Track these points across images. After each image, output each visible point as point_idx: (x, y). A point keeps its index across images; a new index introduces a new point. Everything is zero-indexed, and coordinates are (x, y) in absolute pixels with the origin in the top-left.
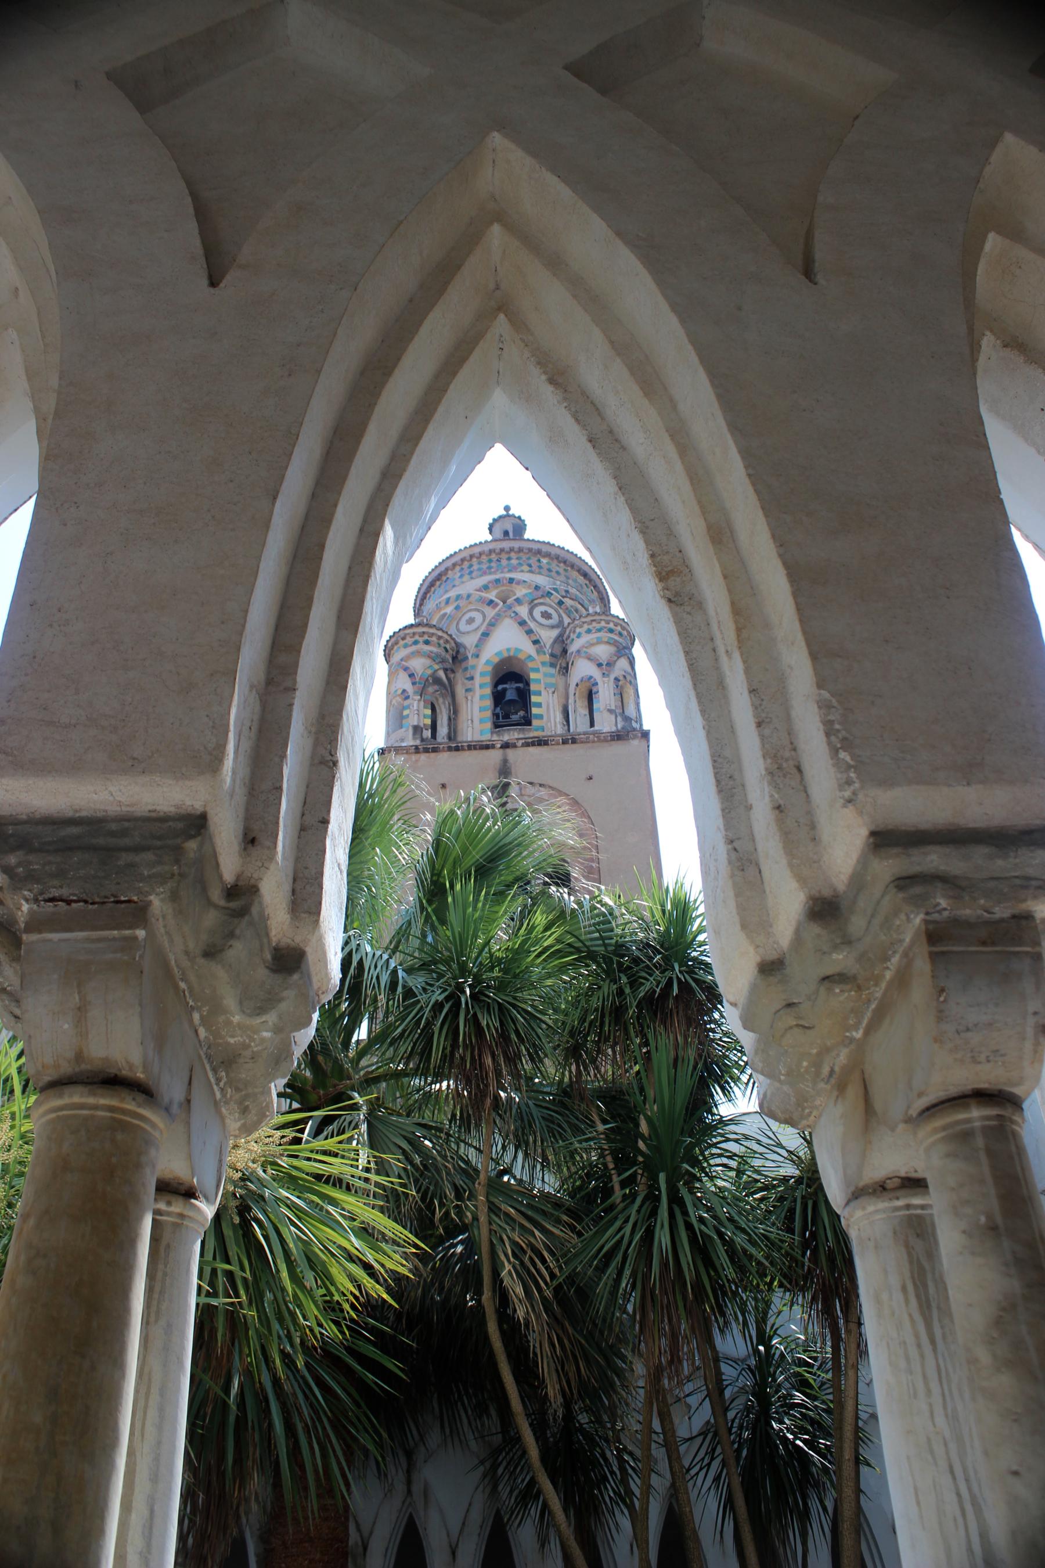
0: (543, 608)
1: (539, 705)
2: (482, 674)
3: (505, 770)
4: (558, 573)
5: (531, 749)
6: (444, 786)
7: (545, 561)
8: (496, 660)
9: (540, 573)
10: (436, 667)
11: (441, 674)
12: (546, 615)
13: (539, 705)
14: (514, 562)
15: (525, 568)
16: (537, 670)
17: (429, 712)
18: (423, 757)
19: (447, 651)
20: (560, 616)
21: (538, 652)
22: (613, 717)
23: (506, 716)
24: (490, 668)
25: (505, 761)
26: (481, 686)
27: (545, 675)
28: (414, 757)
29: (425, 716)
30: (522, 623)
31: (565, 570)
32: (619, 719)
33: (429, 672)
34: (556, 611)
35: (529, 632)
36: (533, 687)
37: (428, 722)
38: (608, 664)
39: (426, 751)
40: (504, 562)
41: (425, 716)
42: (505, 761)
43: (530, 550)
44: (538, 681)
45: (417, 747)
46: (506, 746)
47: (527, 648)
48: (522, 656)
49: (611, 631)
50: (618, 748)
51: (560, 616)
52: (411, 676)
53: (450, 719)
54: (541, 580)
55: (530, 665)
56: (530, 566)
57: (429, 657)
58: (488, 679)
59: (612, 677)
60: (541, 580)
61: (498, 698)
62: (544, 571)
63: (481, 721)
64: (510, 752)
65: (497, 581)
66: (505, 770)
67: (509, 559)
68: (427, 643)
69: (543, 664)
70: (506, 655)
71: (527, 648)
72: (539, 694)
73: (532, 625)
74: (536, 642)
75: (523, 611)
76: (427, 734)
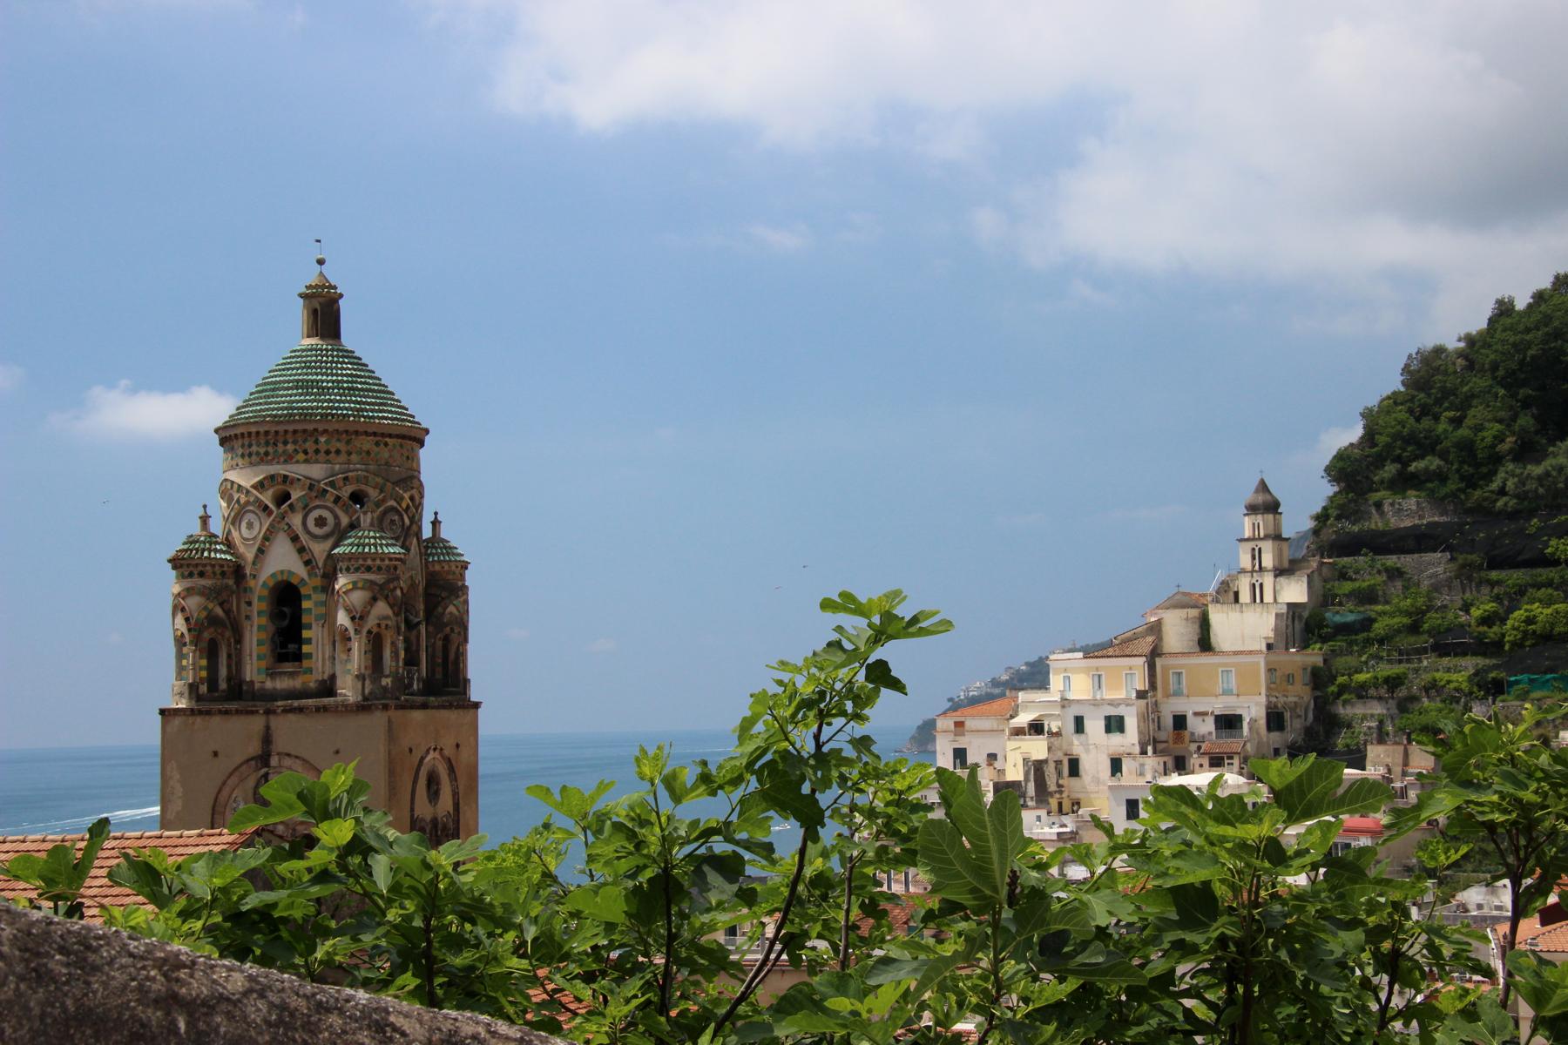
0: (316, 514)
1: (309, 641)
2: (260, 598)
3: (267, 739)
4: (338, 452)
5: (292, 717)
6: (216, 754)
7: (323, 439)
8: (271, 584)
9: (317, 462)
10: (211, 606)
11: (219, 611)
12: (320, 522)
13: (309, 641)
14: (290, 447)
15: (301, 456)
16: (309, 597)
17: (204, 662)
18: (199, 719)
19: (223, 574)
20: (336, 517)
21: (309, 575)
22: (359, 685)
23: (283, 645)
24: (266, 593)
25: (268, 728)
26: (259, 613)
27: (316, 604)
28: (191, 719)
29: (201, 668)
30: (295, 539)
31: (348, 442)
32: (367, 682)
33: (204, 614)
34: (332, 511)
35: (301, 550)
36: (305, 619)
37: (204, 674)
38: (361, 618)
39: (200, 712)
40: (281, 448)
41: (201, 668)
42: (268, 728)
43: (305, 431)
44: (310, 610)
45: (192, 710)
46: (268, 712)
47: (300, 570)
48: (295, 581)
49: (369, 569)
50: (364, 720)
51: (336, 517)
52: (187, 620)
53: (229, 656)
54: (316, 471)
55: (303, 591)
56: (306, 452)
57: (202, 594)
58: (264, 606)
59: (365, 631)
60: (316, 471)
61: (276, 615)
62: (322, 456)
63: (259, 658)
64: (272, 717)
65: (272, 477)
66: (267, 739)
67: (285, 443)
68: (201, 575)
69: (315, 589)
70: (280, 578)
71: (300, 570)
72: (309, 627)
73: (304, 538)
74: (307, 563)
75: (296, 520)
76: (204, 689)
